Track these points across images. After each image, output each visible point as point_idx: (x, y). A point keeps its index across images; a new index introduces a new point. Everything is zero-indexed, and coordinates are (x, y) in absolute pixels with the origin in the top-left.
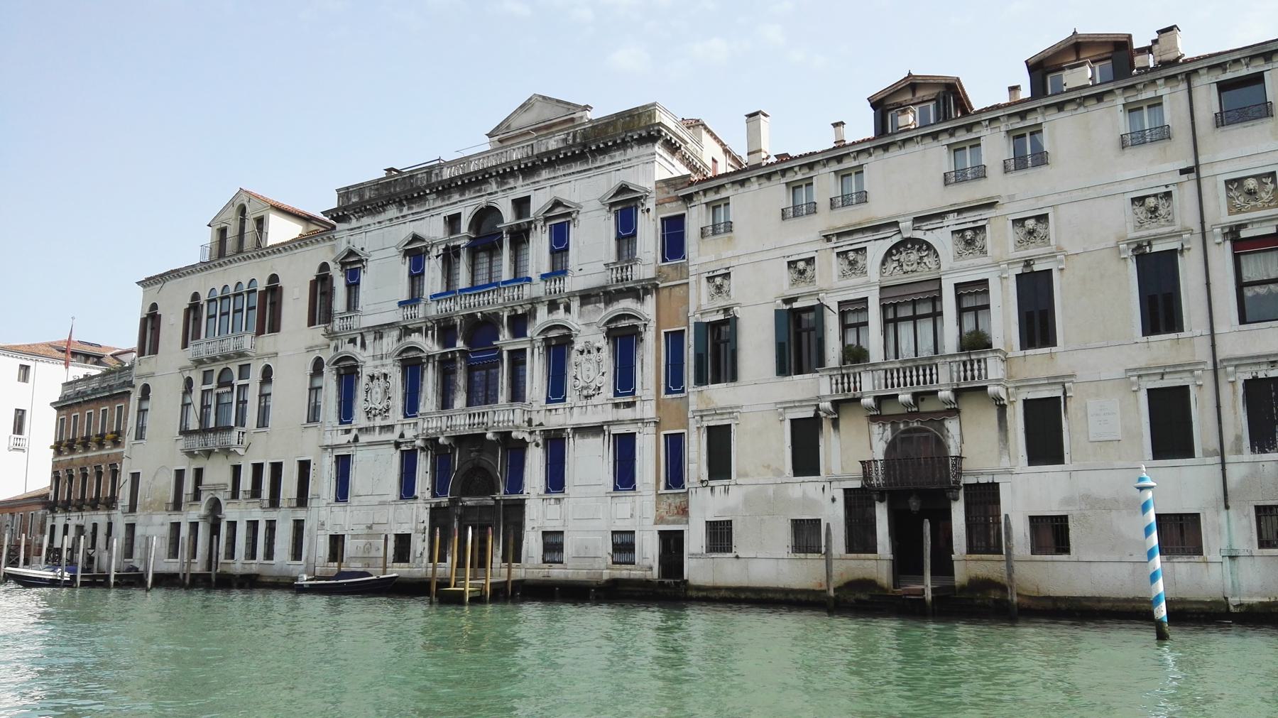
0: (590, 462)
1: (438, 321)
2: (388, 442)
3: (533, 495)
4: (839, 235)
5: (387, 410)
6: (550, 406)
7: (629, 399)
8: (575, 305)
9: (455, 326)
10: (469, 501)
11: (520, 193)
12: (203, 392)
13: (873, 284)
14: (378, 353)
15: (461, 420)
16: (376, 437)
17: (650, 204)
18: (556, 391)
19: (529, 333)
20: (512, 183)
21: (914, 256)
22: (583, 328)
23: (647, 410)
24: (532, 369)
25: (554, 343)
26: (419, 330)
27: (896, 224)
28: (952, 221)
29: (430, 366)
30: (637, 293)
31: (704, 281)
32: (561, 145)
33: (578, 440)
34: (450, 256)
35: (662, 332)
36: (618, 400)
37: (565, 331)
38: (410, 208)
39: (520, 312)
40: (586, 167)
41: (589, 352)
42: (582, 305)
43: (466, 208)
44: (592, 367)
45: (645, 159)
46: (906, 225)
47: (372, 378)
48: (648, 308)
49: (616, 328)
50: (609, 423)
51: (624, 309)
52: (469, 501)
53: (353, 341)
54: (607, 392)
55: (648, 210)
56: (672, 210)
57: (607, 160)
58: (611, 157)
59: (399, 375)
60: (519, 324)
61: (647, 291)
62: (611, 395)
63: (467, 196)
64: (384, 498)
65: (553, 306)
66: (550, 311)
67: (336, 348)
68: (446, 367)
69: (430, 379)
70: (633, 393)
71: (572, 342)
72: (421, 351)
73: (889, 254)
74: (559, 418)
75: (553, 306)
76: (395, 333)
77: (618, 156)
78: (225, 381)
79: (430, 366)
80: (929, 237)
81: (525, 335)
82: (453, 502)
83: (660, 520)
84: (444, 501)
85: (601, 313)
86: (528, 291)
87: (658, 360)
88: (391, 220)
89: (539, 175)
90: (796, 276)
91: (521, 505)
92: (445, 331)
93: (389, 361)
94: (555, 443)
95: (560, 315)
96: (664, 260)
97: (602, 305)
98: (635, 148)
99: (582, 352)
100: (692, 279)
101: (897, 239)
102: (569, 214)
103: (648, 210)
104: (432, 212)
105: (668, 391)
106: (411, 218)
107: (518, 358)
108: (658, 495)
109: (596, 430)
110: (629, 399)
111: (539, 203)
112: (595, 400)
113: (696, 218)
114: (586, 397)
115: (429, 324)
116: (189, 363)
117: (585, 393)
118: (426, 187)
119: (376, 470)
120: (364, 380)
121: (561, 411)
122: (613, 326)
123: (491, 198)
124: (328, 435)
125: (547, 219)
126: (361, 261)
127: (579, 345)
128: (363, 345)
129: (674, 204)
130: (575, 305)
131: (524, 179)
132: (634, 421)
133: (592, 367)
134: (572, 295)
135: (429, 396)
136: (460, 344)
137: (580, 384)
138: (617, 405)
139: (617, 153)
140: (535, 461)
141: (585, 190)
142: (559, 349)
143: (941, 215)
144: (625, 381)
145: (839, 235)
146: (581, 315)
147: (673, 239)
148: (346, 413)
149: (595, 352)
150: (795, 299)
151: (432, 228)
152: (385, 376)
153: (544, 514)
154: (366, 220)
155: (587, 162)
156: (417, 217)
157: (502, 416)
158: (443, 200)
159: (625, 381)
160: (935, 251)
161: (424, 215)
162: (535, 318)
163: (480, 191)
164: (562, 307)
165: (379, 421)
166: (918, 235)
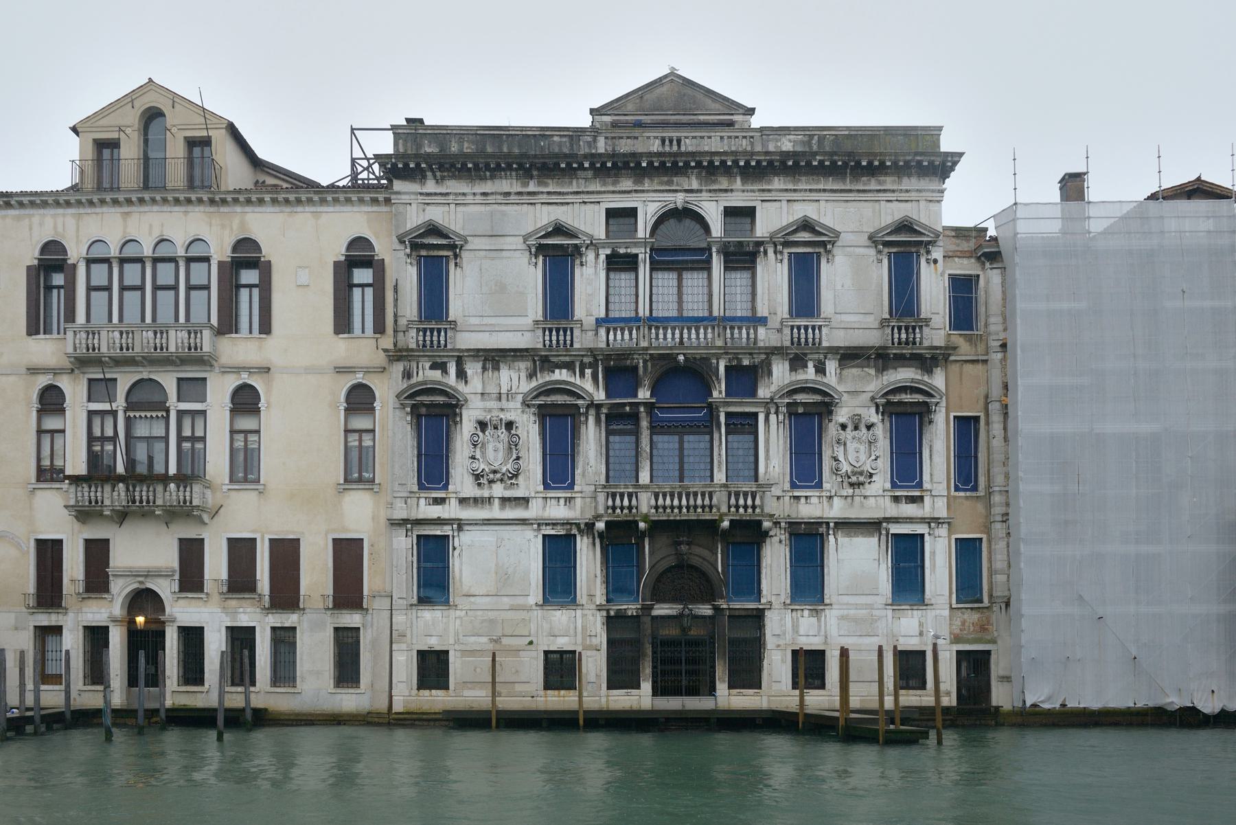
0: (856, 563)
1: (608, 357)
2: (523, 522)
3: (776, 604)
5: (516, 476)
8: (831, 366)
9: (636, 368)
10: (662, 610)
12: (91, 414)
14: (492, 389)
16: (496, 512)
17: (937, 253)
18: (806, 469)
20: (724, 183)
23: (935, 506)
25: (801, 410)
26: (569, 366)
29: (591, 420)
32: (799, 149)
35: (952, 415)
37: (827, 399)
38: (540, 184)
39: (746, 362)
41: (856, 428)
43: (649, 207)
44: (858, 448)
45: (929, 195)
47: (482, 425)
49: (900, 403)
51: (905, 380)
52: (662, 610)
53: (443, 367)
54: (881, 482)
55: (935, 261)
56: (966, 267)
57: (873, 185)
58: (880, 183)
59: (534, 430)
60: (745, 377)
62: (888, 485)
63: (646, 186)
64: (520, 601)
65: (797, 362)
66: (793, 369)
67: (407, 375)
68: (619, 420)
69: (591, 438)
70: (920, 485)
71: (830, 413)
72: (580, 397)
75: (797, 362)
77: (889, 182)
78: (146, 399)
79: (591, 420)
82: (647, 609)
83: (956, 639)
85: (874, 383)
86: (765, 336)
88: (508, 194)
89: (770, 182)
91: (758, 617)
93: (517, 403)
97: (872, 371)
98: (914, 180)
99: (844, 427)
102: (824, 244)
103: (935, 261)
104: (586, 198)
106: (544, 198)
107: (744, 425)
108: (951, 608)
109: (873, 526)
111: (771, 218)
114: (852, 485)
115: (586, 360)
116: (66, 363)
117: (854, 479)
118: (585, 157)
119: (497, 561)
120: (467, 426)
121: (814, 500)
122: (896, 398)
123: (691, 197)
124: (399, 504)
125: (787, 244)
126: (453, 247)
127: (842, 415)
128: (461, 375)
129: (965, 261)
130: (831, 366)
131: (744, 182)
133: (858, 448)
134: (833, 350)
135: (592, 462)
136: (644, 394)
137: (845, 467)
138: (896, 499)
139: (889, 179)
142: (810, 418)
144: (906, 469)
146: (841, 379)
148: (433, 470)
149: (864, 430)
151: (589, 220)
152: (510, 425)
154: (453, 186)
155: (844, 179)
156: (554, 199)
158: (604, 184)
159: (906, 469)
161: (570, 198)
162: (770, 373)
163: (670, 183)
164: (810, 365)
165: (498, 490)
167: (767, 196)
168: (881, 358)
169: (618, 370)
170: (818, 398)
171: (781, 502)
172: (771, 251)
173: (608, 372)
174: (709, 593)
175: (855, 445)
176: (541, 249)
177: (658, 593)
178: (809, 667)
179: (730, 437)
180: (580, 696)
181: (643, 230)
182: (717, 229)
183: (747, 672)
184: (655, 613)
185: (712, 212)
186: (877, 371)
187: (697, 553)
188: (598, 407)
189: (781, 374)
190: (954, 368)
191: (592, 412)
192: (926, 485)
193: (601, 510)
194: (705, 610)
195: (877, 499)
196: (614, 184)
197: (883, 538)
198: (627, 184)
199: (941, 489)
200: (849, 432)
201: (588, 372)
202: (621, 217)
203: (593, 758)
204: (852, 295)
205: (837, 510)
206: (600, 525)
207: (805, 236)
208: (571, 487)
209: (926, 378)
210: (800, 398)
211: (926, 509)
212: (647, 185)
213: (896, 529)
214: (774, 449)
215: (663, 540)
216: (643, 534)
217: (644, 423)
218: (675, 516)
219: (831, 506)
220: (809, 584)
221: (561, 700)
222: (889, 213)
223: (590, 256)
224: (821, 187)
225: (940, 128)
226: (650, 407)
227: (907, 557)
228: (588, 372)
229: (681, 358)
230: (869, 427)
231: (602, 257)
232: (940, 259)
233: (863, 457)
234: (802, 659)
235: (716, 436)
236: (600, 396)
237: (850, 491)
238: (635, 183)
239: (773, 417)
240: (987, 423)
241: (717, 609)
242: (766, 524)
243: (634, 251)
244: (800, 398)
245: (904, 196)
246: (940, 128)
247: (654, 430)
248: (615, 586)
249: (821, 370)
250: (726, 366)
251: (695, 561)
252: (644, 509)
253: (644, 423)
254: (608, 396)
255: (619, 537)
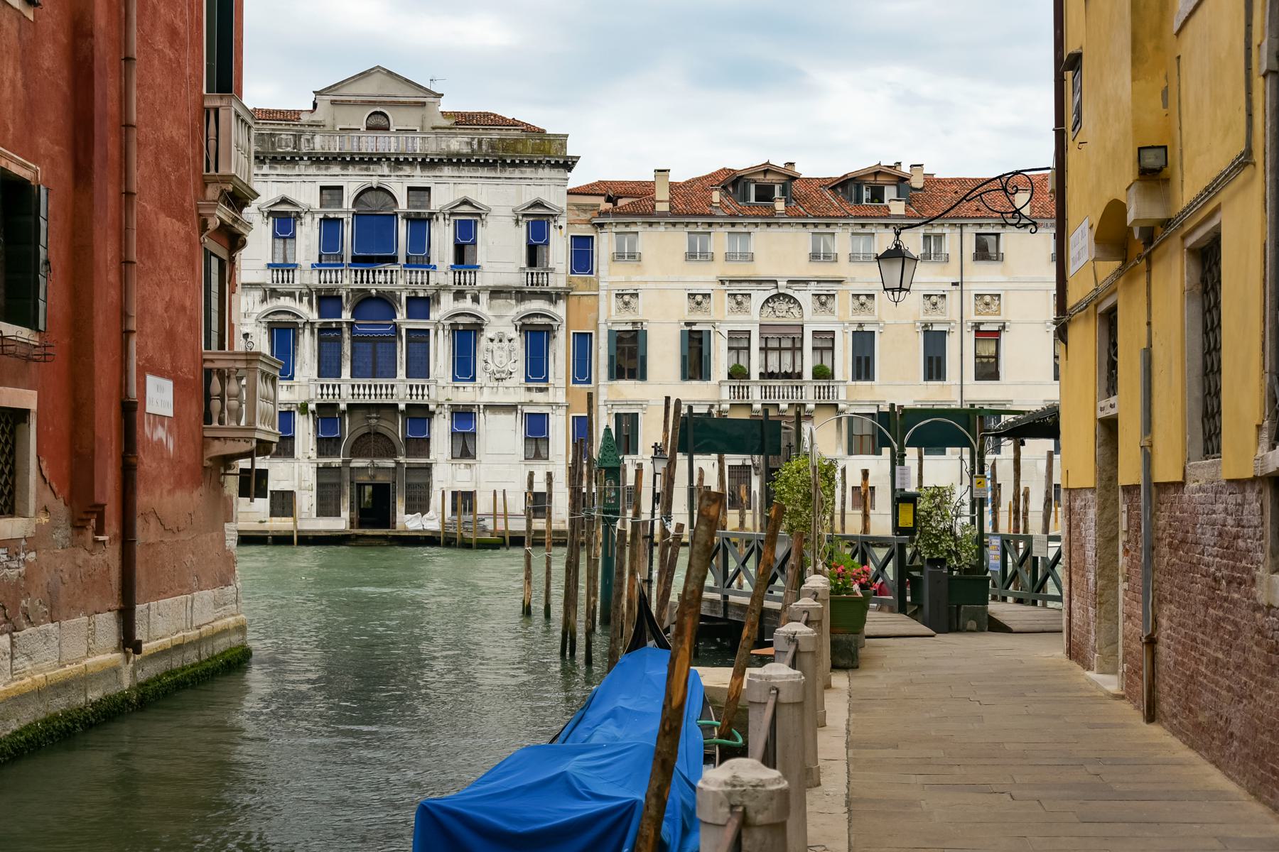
0: (500, 436)
1: (318, 290)
4: (731, 281)
6: (457, 384)
7: (543, 385)
8: (484, 297)
9: (340, 297)
11: (418, 182)
13: (755, 322)
15: (347, 389)
17: (562, 222)
18: (464, 368)
19: (432, 315)
20: (407, 170)
21: (785, 307)
22: (493, 319)
23: (557, 394)
24: (436, 349)
25: (461, 328)
27: (776, 282)
28: (813, 286)
30: (552, 297)
31: (613, 296)
33: (489, 415)
34: (330, 226)
36: (531, 385)
39: (421, 294)
40: (493, 174)
42: (491, 298)
43: (352, 182)
46: (782, 283)
48: (560, 310)
49: (531, 325)
50: (523, 404)
54: (519, 377)
56: (584, 231)
60: (420, 305)
61: (559, 296)
65: (459, 295)
68: (328, 337)
69: (307, 347)
70: (546, 380)
72: (298, 317)
73: (767, 301)
74: (466, 395)
76: (258, 294)
77: (529, 172)
79: (307, 332)
80: (796, 295)
81: (428, 318)
84: (336, 461)
85: (515, 310)
87: (567, 355)
89: (441, 170)
90: (694, 305)
91: (428, 469)
92: (327, 300)
93: (252, 320)
94: (463, 416)
95: (467, 304)
96: (572, 272)
97: (513, 302)
98: (547, 170)
99: (492, 340)
100: (602, 293)
101: (774, 292)
102: (479, 215)
105: (575, 382)
107: (419, 339)
109: (511, 408)
110: (543, 385)
112: (507, 383)
113: (605, 245)
115: (304, 291)
117: (498, 376)
121: (470, 389)
122: (527, 321)
123: (383, 180)
125: (452, 214)
127: (489, 332)
130: (484, 297)
132: (549, 404)
134: (485, 288)
135: (307, 361)
136: (346, 316)
137: (491, 367)
138: (529, 389)
139: (528, 170)
140: (441, 430)
141: (501, 197)
143: (806, 282)
145: (731, 281)
146: (490, 308)
147: (582, 254)
149: (506, 343)
150: (694, 324)
153: (453, 477)
155: (495, 170)
156: (281, 179)
157: (401, 390)
158: (319, 169)
159: (537, 369)
160: (800, 306)
162: (439, 302)
163: (367, 169)
164: (469, 296)
166: (789, 292)
167: (438, 180)
168: (521, 295)
169: (327, 300)
170: (473, 320)
171: (441, 385)
172: (441, 218)
173: (320, 298)
174: (391, 452)
175: (500, 352)
176: (271, 213)
177: (356, 451)
178: (464, 500)
179: (411, 345)
180: (295, 522)
181: (348, 203)
182: (403, 206)
183: (419, 503)
184: (352, 465)
185: (399, 188)
186: (517, 301)
187: (384, 426)
188: (312, 324)
189: (447, 305)
190: (574, 299)
191: (308, 327)
192: (551, 380)
193: (313, 396)
194: (390, 463)
195: (515, 391)
196: (327, 169)
197: (519, 416)
198: (336, 169)
199: (562, 382)
200: (496, 344)
201: (305, 299)
202: (331, 193)
203: (306, 558)
204: (500, 252)
205: (486, 397)
206: (312, 407)
207: (466, 209)
208: (292, 378)
209: (552, 308)
210: (460, 320)
211: (550, 397)
212: (351, 170)
213: (528, 410)
214: (441, 353)
215: (359, 415)
216: (344, 412)
217: (346, 335)
218: (367, 400)
219: (482, 394)
220: (465, 446)
221: (282, 524)
222: (529, 194)
223: (308, 218)
224: (478, 174)
225: (567, 136)
226: (351, 325)
227: (536, 428)
228: (305, 299)
229: (374, 292)
230: (510, 341)
231: (317, 220)
232: (564, 226)
233: (505, 360)
234: (459, 498)
235: (399, 344)
236: (314, 316)
237: (496, 384)
238: (343, 169)
239: (440, 332)
240: (597, 338)
241: (398, 463)
242: (432, 407)
243: (340, 216)
244: (460, 320)
245: (539, 182)
246: (567, 136)
247: (354, 340)
248: (326, 445)
249: (476, 299)
250: (407, 298)
251: (381, 430)
252: (344, 395)
253: (346, 335)
254: (320, 317)
255: (326, 414)
